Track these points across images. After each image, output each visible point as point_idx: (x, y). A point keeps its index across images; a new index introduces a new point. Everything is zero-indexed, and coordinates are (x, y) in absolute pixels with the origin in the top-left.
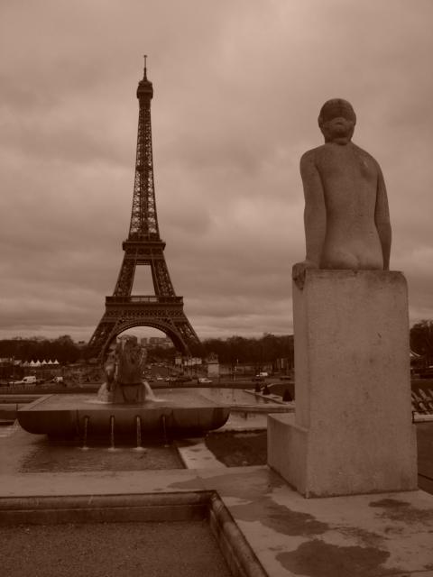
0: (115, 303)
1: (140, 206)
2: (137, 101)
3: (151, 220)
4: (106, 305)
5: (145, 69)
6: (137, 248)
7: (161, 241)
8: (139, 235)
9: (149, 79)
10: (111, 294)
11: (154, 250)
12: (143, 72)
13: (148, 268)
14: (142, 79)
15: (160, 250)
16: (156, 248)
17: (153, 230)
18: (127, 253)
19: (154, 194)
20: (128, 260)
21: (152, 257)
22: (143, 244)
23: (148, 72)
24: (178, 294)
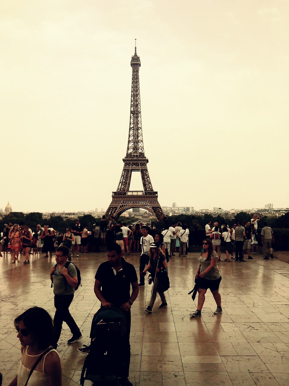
0: (117, 196)
1: (133, 136)
2: (130, 69)
3: (140, 144)
5: (136, 48)
6: (131, 162)
8: (133, 154)
9: (138, 55)
10: (115, 191)
11: (141, 163)
14: (134, 54)
16: (142, 162)
17: (140, 151)
18: (125, 165)
21: (140, 167)
22: (134, 160)
24: (155, 191)
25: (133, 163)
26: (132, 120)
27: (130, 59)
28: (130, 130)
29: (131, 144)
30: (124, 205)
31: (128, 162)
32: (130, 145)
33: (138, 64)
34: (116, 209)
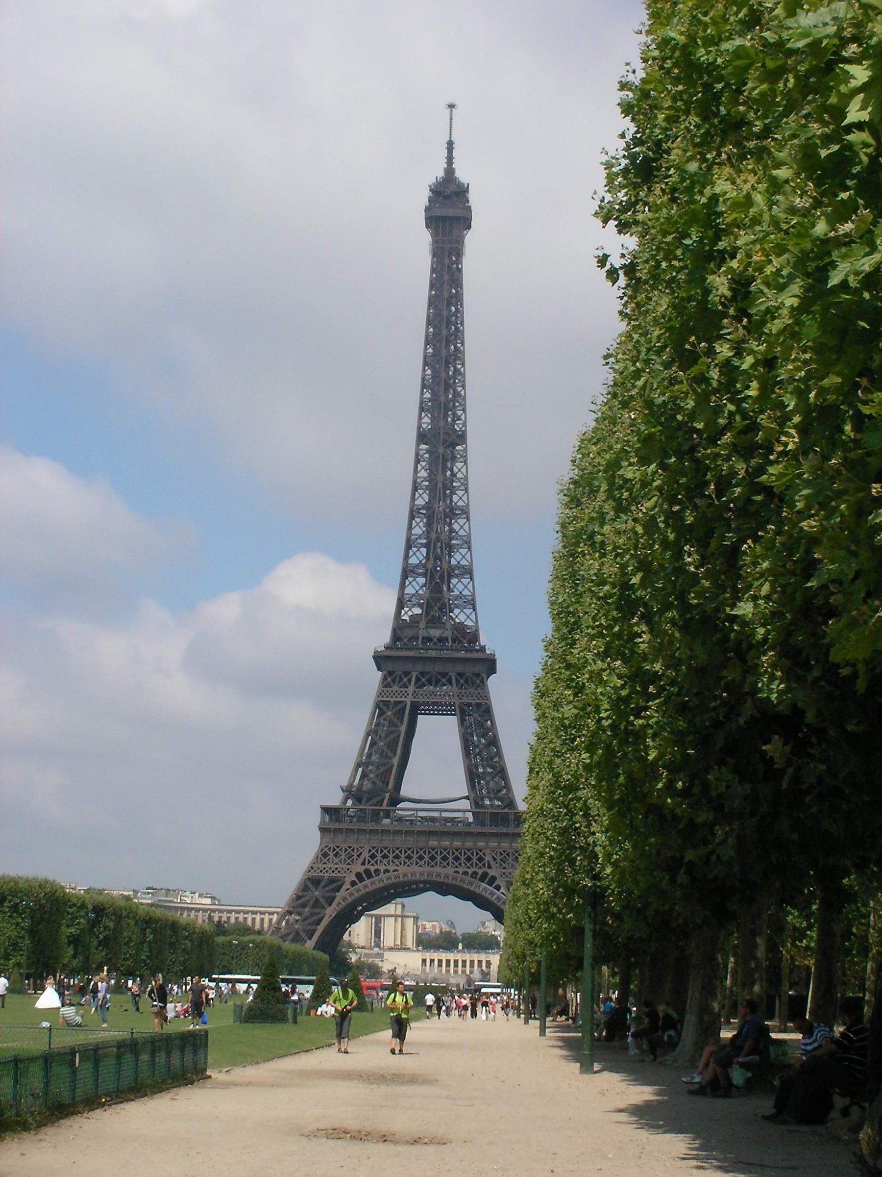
1: (427, 546)
3: (459, 586)
4: (323, 830)
5: (450, 145)
7: (483, 649)
8: (422, 633)
9: (462, 175)
10: (335, 799)
12: (445, 153)
13: (450, 724)
14: (441, 174)
15: (478, 675)
16: (469, 670)
17: (460, 616)
18: (385, 684)
19: (465, 512)
20: (386, 704)
23: (455, 153)
25: (422, 674)
26: (423, 474)
27: (423, 197)
28: (412, 517)
29: (417, 585)
30: (377, 871)
31: (399, 668)
32: (409, 590)
33: (458, 218)
34: (338, 889)
